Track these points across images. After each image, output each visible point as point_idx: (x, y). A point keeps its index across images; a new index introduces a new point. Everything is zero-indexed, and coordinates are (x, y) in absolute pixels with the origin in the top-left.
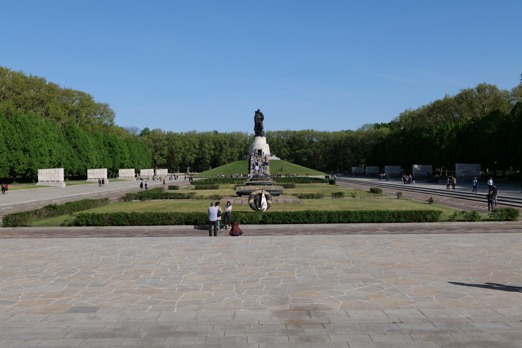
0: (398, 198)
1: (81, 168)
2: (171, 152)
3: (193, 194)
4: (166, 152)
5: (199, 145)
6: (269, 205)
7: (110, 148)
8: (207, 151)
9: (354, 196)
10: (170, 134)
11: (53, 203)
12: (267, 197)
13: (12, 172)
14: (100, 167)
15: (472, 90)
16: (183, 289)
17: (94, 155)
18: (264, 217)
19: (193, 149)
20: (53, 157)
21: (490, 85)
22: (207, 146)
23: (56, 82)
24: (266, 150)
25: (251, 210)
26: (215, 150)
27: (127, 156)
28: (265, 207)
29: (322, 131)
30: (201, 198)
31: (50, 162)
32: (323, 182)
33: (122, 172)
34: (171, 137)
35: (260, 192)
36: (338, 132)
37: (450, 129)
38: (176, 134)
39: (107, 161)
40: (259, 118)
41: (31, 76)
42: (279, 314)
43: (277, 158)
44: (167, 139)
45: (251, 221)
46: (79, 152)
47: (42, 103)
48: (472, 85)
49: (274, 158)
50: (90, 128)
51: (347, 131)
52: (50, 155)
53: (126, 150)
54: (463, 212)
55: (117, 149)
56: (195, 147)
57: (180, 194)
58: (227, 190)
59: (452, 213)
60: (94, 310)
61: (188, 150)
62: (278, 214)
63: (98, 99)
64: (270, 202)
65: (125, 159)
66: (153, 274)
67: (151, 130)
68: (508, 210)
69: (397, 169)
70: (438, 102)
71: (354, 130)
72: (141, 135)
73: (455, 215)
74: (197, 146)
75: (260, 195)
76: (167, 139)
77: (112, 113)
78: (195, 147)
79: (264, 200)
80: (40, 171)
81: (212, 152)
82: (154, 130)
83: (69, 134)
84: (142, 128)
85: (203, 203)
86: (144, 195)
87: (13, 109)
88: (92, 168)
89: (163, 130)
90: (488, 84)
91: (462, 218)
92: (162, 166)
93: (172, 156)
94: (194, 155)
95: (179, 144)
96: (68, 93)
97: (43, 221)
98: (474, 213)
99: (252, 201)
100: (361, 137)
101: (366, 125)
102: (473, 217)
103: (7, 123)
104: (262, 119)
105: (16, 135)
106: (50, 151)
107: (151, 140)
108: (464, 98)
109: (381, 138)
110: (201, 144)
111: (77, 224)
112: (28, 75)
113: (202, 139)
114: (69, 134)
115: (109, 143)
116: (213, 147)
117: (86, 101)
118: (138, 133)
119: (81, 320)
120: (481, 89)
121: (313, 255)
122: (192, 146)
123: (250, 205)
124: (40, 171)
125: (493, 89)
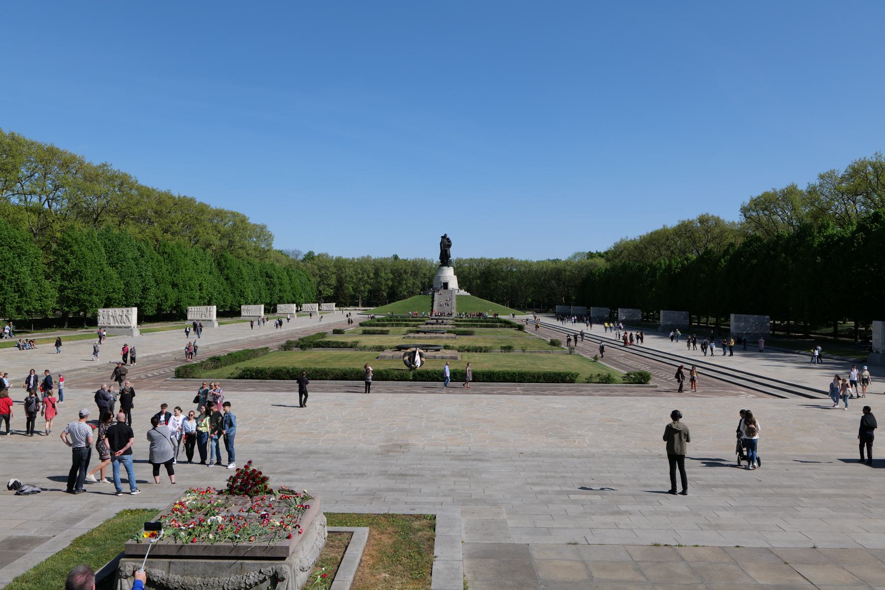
0: (571, 353)
1: (234, 303)
2: (340, 281)
3: (357, 342)
4: (333, 281)
5: (374, 274)
6: (422, 363)
7: (268, 279)
8: (384, 283)
9: (524, 351)
10: (339, 260)
11: (217, 355)
12: (421, 355)
13: (159, 308)
14: (255, 303)
15: (691, 222)
16: (327, 432)
17: (250, 289)
18: (414, 375)
19: (366, 278)
20: (204, 291)
21: (713, 216)
22: (383, 274)
23: (207, 203)
24: (453, 284)
25: (405, 367)
26: (392, 279)
27: (288, 288)
28: (418, 364)
29: (524, 259)
30: (364, 348)
31: (200, 298)
32: (511, 327)
33: (280, 307)
34: (340, 264)
35: (414, 349)
36: (544, 262)
37: (663, 266)
38: (346, 260)
39: (264, 295)
40: (446, 244)
41: (179, 197)
42: (381, 447)
43: (466, 293)
44: (335, 266)
45: (402, 378)
46: (232, 284)
47: (190, 226)
48: (691, 215)
49: (463, 292)
50: (245, 255)
51: (555, 261)
52: (200, 290)
53: (286, 280)
54: (599, 375)
55: (276, 280)
56: (368, 277)
57: (343, 343)
58: (395, 338)
59: (588, 376)
60: (270, 442)
61: (360, 279)
62: (427, 372)
63: (254, 219)
64: (423, 359)
65: (285, 291)
66: (307, 422)
67: (316, 254)
68: (641, 374)
69: (605, 312)
70: (656, 233)
71: (563, 259)
72: (304, 260)
73: (591, 377)
74: (372, 275)
75: (415, 352)
76: (335, 266)
77: (270, 235)
78: (368, 277)
79: (417, 358)
80: (190, 308)
81: (390, 283)
82: (319, 255)
83: (221, 264)
84: (306, 252)
85: (363, 356)
86: (306, 343)
87: (159, 234)
88: (246, 303)
89: (330, 255)
90: (710, 215)
91: (598, 380)
92: (328, 300)
93: (341, 287)
94: (368, 286)
95: (349, 271)
96: (220, 214)
97: (209, 373)
98: (609, 376)
99: (406, 358)
100: (569, 268)
101: (578, 254)
102: (607, 380)
103: (156, 255)
104: (449, 246)
105: (164, 268)
106: (200, 285)
107: (316, 267)
108: (684, 230)
109: (591, 274)
110: (377, 274)
111: (241, 377)
112: (176, 195)
113: (378, 267)
114: (221, 264)
115: (267, 273)
116: (391, 276)
117: (240, 223)
118: (301, 258)
119: (263, 447)
120: (703, 220)
121: (432, 411)
122: (365, 275)
123: (405, 362)
124: (190, 308)
125: (717, 221)
